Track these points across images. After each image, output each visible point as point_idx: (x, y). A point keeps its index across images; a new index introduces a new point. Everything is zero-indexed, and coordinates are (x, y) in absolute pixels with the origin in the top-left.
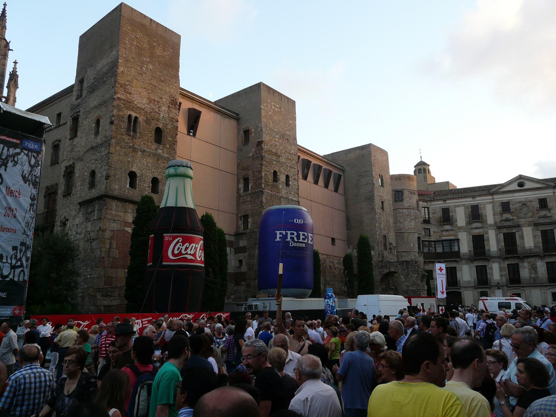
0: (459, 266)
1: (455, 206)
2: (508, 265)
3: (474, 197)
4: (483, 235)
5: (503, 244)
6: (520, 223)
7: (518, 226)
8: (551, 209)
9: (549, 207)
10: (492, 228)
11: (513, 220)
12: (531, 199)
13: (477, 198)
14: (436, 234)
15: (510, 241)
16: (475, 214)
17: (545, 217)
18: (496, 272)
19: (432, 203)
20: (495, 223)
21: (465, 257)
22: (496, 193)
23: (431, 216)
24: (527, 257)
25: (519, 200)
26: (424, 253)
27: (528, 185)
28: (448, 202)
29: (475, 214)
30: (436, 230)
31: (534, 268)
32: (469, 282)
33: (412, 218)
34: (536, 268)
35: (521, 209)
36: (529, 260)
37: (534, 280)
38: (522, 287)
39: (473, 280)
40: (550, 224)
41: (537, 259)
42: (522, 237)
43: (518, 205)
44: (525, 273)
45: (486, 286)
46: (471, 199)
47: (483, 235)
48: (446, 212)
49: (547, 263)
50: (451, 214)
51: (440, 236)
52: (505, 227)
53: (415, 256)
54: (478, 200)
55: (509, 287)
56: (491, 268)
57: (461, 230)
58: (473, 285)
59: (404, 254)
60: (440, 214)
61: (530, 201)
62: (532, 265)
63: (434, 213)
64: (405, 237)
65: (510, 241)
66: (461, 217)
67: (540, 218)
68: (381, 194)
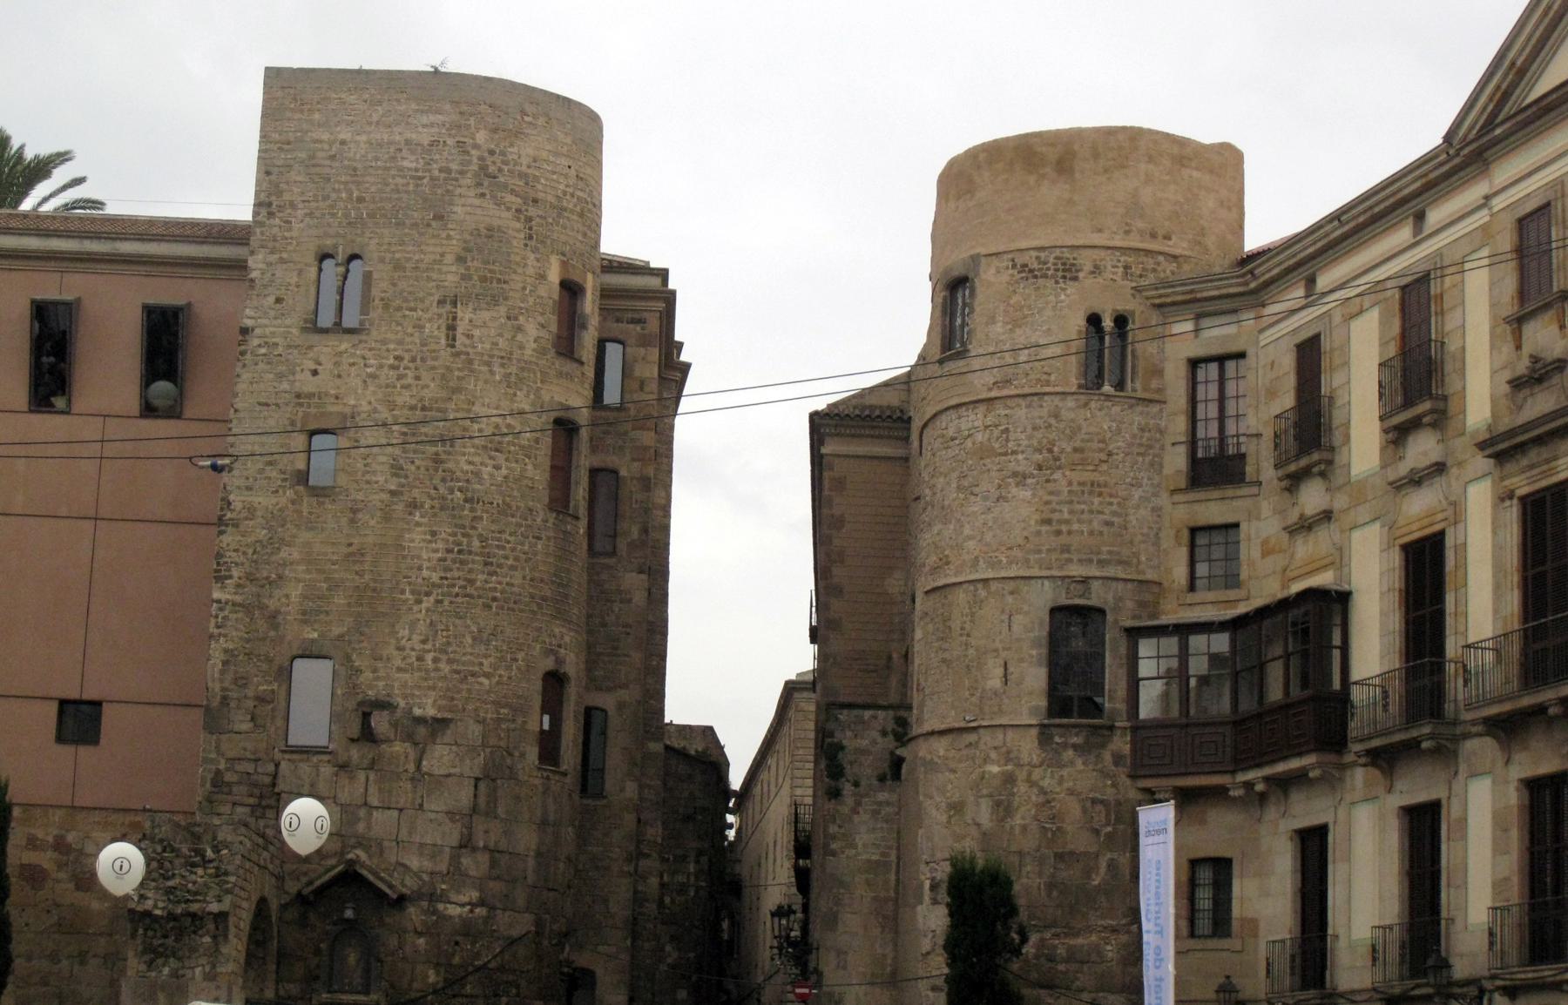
5: (1513, 601)
13: (1435, 217)
14: (1270, 560)
26: (1138, 728)
33: (1021, 463)
46: (1404, 234)
53: (1008, 757)
57: (1363, 513)
59: (940, 746)
64: (956, 624)
68: (307, 383)
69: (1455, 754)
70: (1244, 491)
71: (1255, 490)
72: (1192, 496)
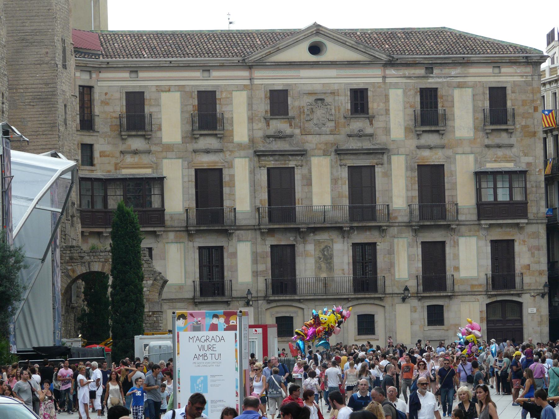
0: (160, 245)
1: (160, 89)
2: (272, 247)
3: (206, 69)
4: (221, 170)
5: (265, 196)
6: (308, 146)
7: (302, 154)
8: (374, 117)
9: (370, 111)
10: (242, 153)
11: (291, 136)
12: (336, 87)
13: (215, 74)
14: (105, 160)
15: (281, 189)
16: (207, 115)
17: (360, 135)
18: (245, 264)
19: (103, 75)
20: (252, 141)
21: (176, 224)
22: (260, 64)
23: (97, 109)
24: (315, 230)
25: (309, 88)
27: (333, 52)
28: (141, 74)
29: (207, 115)
30: (107, 148)
31: (326, 258)
32: (181, 287)
34: (331, 257)
35: (312, 111)
36: (318, 237)
37: (325, 285)
38: (299, 301)
39: (190, 282)
40: (370, 153)
41: (334, 235)
42: (308, 182)
43: (306, 101)
44: (306, 268)
45: (219, 299)
46: (197, 74)
47: (221, 170)
48: (135, 100)
49: (354, 245)
50: (147, 110)
51: (117, 167)
52: (273, 154)
54: (216, 80)
55: (269, 302)
56: (234, 255)
57: (169, 154)
58: (190, 295)
60: (119, 107)
61: (333, 93)
62: (323, 250)
63: (105, 103)
65: (281, 189)
66: (171, 117)
67: (350, 136)
69: (231, 234)
70: (95, 134)
71: (97, 134)
72: (83, 133)
